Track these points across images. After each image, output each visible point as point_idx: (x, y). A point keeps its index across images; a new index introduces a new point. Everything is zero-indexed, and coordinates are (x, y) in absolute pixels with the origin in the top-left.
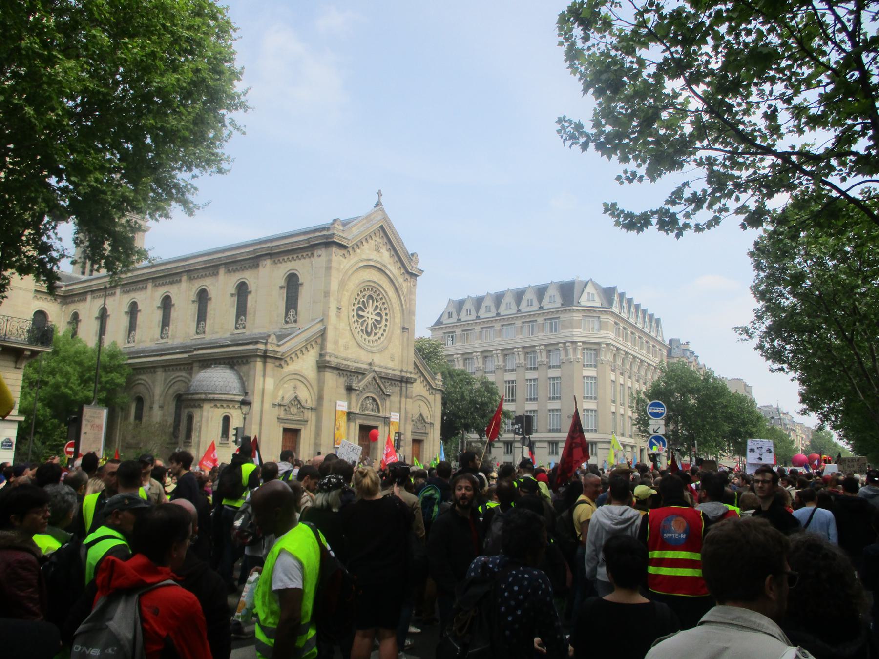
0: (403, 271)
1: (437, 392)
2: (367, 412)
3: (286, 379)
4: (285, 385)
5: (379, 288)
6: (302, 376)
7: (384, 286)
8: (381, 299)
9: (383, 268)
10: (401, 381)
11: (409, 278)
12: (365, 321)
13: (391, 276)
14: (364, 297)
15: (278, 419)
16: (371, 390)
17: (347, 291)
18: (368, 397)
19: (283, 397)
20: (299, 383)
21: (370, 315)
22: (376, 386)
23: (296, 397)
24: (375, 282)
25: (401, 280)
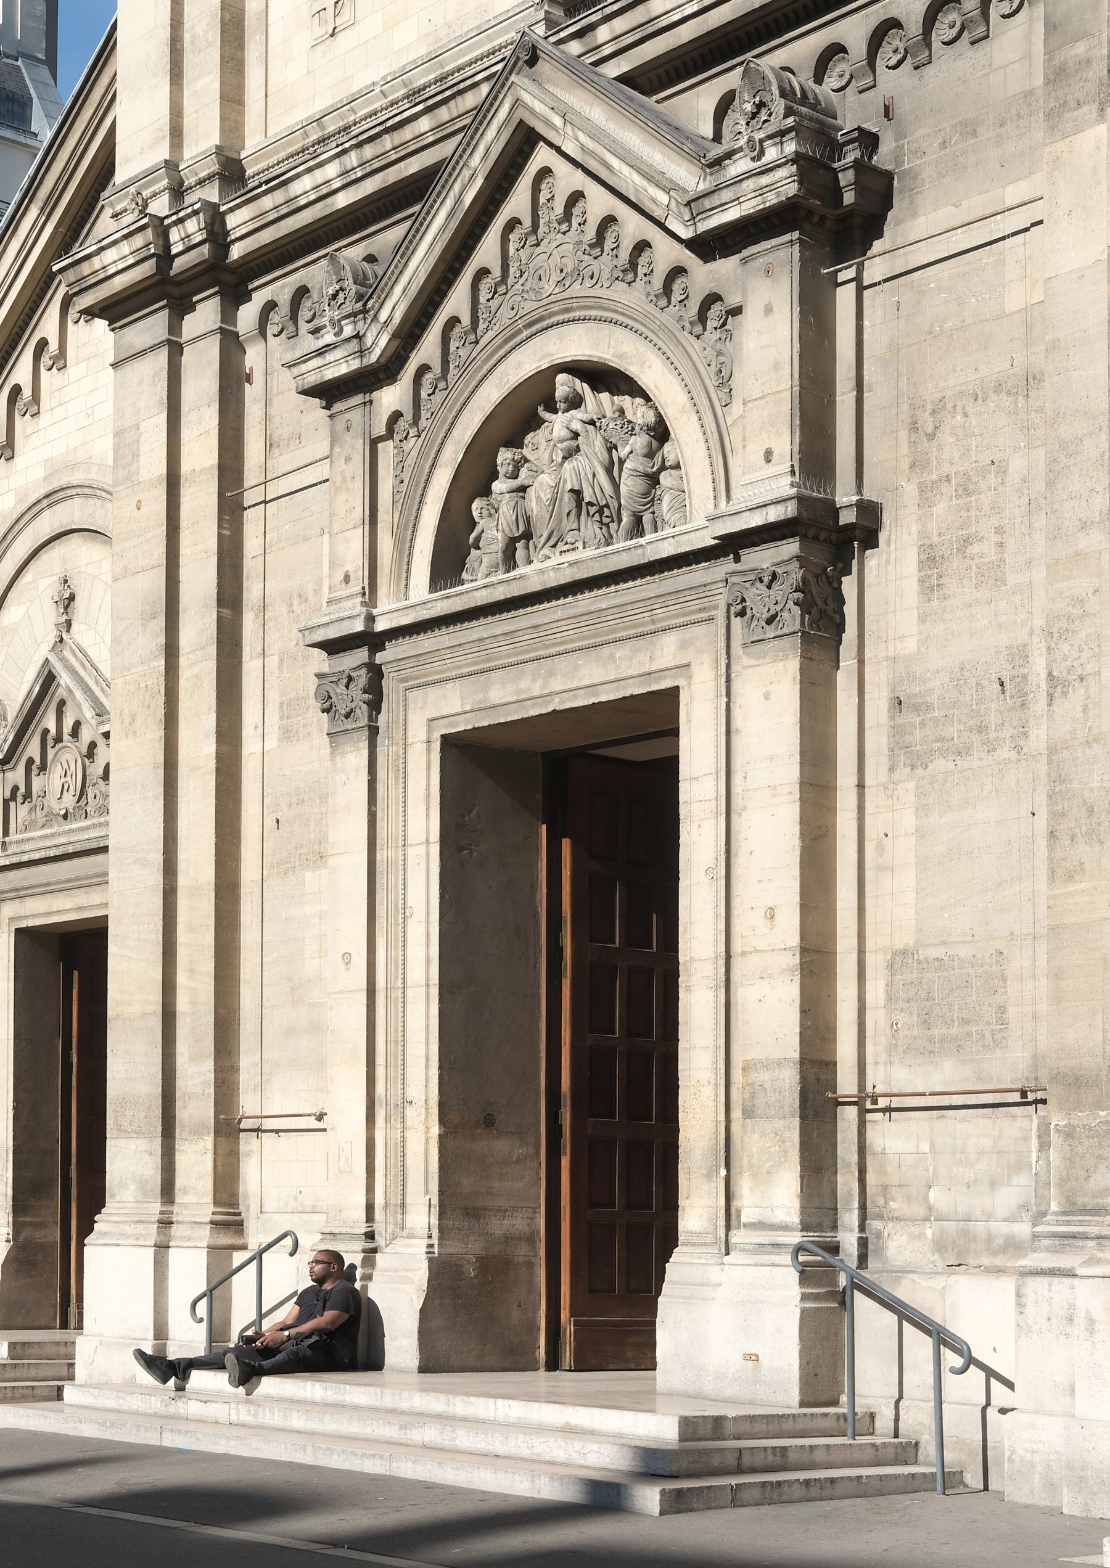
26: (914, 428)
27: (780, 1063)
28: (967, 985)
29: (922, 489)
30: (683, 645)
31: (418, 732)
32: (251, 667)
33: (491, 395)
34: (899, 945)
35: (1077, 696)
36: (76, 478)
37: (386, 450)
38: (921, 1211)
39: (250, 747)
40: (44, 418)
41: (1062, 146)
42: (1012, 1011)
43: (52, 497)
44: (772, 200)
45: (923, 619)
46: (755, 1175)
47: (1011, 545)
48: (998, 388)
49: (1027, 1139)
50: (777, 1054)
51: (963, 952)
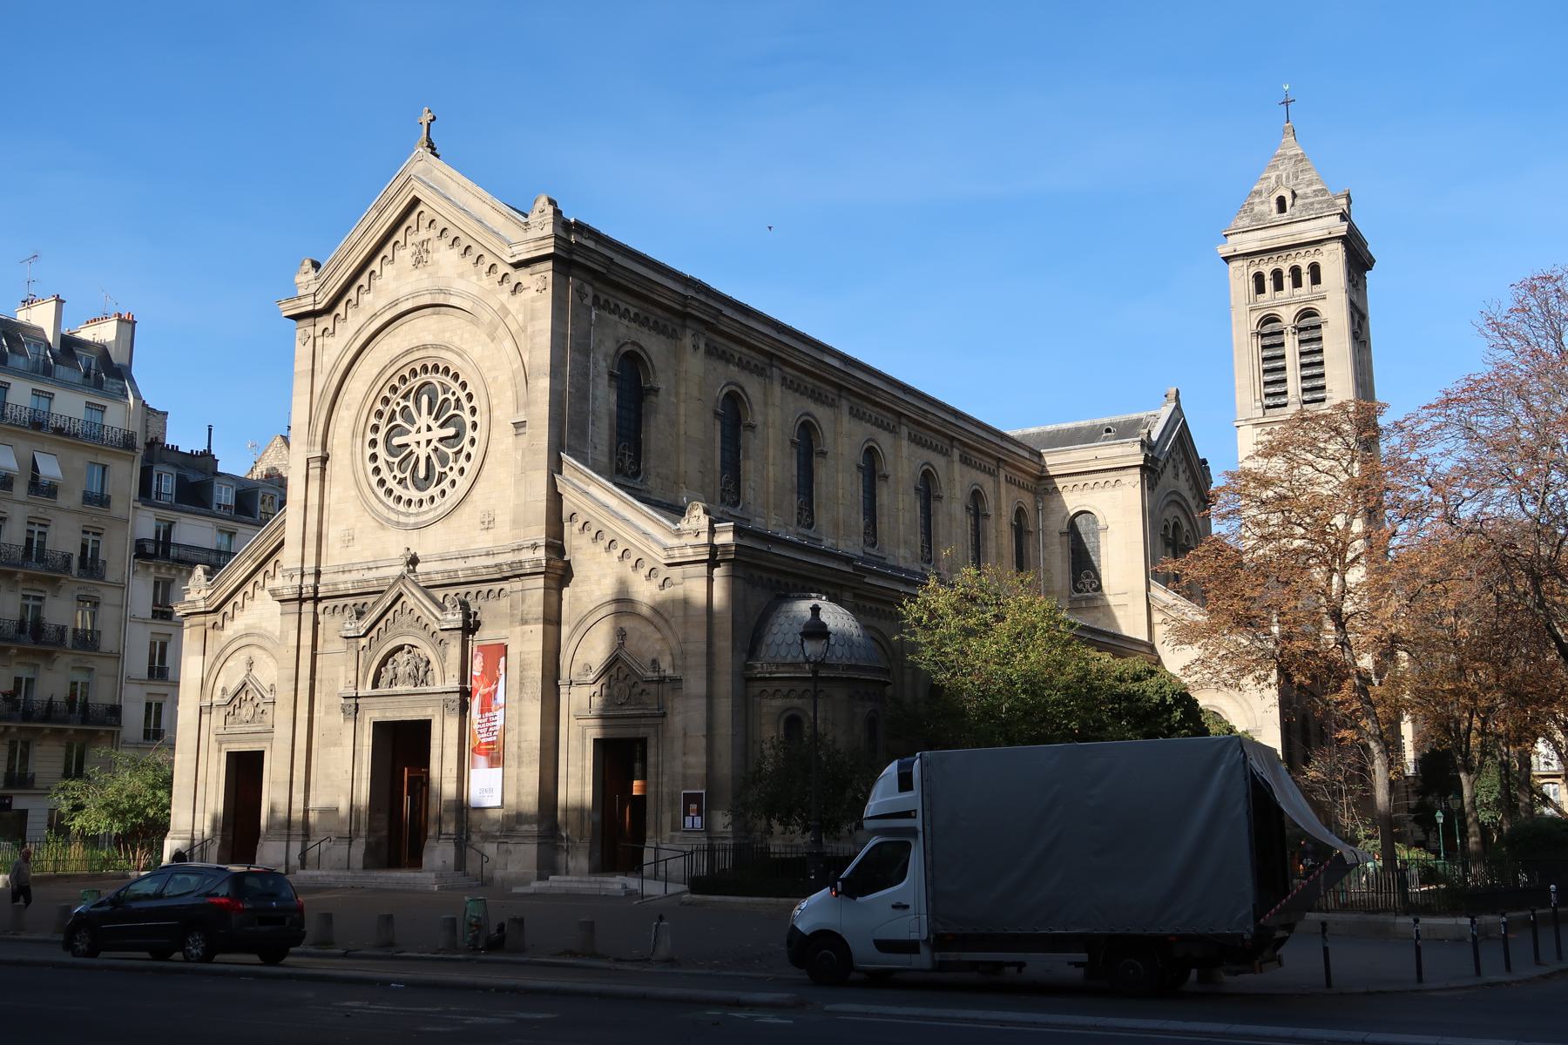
1: (690, 569)
2: (399, 688)
3: (229, 651)
4: (229, 664)
6: (261, 636)
7: (456, 342)
9: (440, 299)
12: (411, 453)
17: (348, 407)
18: (401, 648)
20: (256, 652)
21: (423, 434)
24: (425, 347)
30: (433, 711)
31: (367, 720)
35: (512, 732)
36: (256, 631)
39: (316, 715)
40: (245, 612)
41: (512, 629)
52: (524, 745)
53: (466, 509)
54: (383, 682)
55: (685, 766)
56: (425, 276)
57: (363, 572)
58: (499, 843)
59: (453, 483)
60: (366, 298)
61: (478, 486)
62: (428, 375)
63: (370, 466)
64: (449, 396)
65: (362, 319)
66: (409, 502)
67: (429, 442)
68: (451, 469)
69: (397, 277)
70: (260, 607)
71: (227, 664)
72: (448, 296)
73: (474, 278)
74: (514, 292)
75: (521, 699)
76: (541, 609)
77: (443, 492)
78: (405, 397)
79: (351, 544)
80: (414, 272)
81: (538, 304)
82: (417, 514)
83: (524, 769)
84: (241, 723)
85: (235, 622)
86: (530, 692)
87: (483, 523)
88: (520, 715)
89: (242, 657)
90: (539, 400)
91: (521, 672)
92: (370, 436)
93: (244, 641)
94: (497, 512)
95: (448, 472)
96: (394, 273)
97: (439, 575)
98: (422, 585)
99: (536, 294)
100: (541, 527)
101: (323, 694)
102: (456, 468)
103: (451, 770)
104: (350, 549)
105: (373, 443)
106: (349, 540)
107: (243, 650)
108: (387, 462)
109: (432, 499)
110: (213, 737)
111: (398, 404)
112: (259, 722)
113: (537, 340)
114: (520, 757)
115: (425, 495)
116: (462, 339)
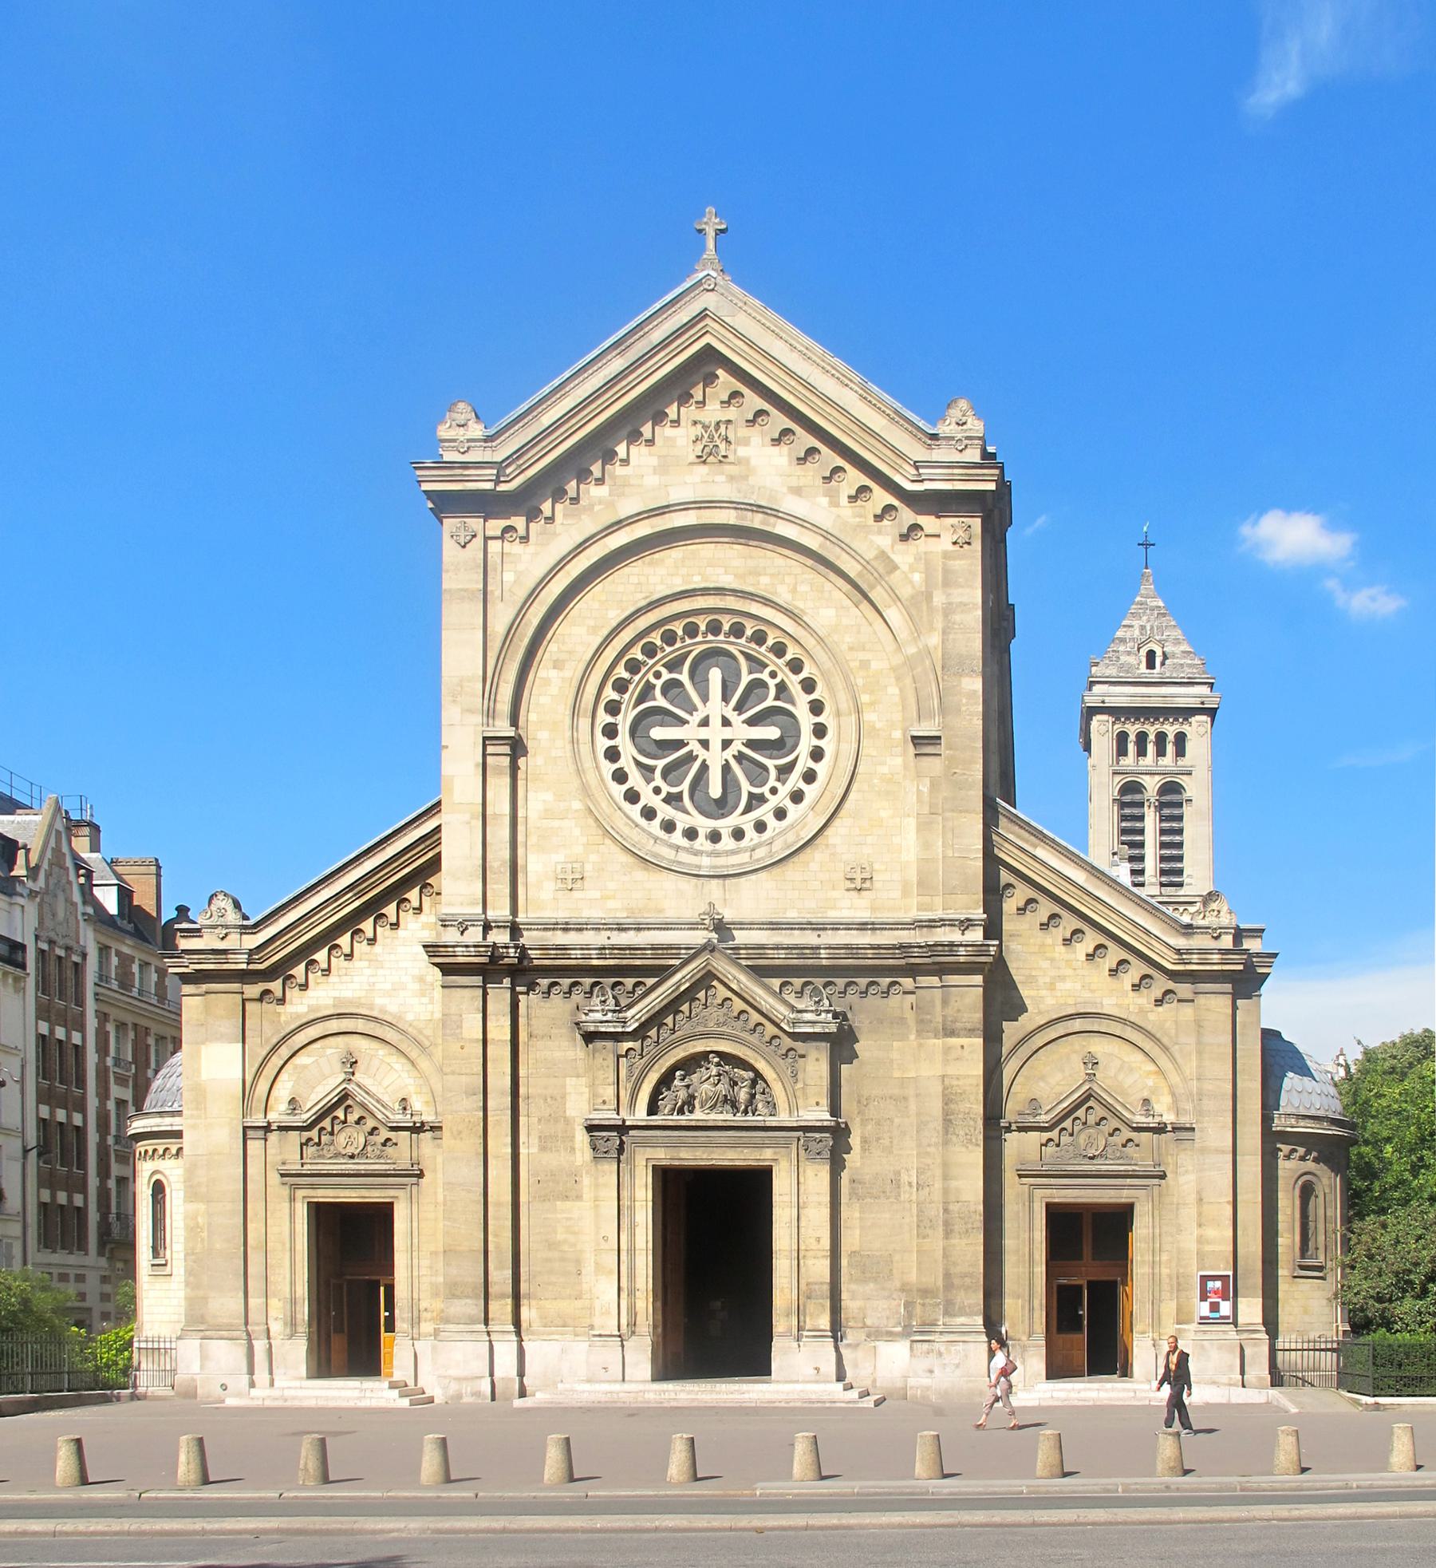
0: (881, 497)
2: (699, 1116)
4: (299, 1060)
5: (755, 608)
6: (375, 1019)
7: (783, 596)
8: (779, 650)
9: (756, 521)
10: (913, 971)
11: (928, 522)
12: (691, 758)
13: (812, 541)
14: (674, 665)
15: (282, 1175)
16: (712, 1027)
17: (557, 665)
18: (705, 1055)
19: (292, 1101)
22: (739, 1005)
23: (345, 1096)
24: (720, 591)
25: (884, 538)
26: (859, 1102)
27: (821, 1283)
28: (878, 1263)
29: (862, 1120)
30: (775, 1153)
31: (640, 1162)
32: (522, 1120)
33: (679, 1053)
34: (854, 1250)
37: (623, 1060)
38: (860, 1325)
39: (523, 1150)
40: (332, 978)
42: (894, 1271)
43: (340, 1016)
44: (827, 1030)
45: (861, 1158)
46: (811, 1315)
47: (895, 1142)
48: (891, 1098)
49: (900, 1305)
50: (821, 1280)
51: (878, 1254)
52: (953, 1207)
53: (815, 857)
54: (665, 1105)
55: (1200, 1240)
56: (722, 478)
57: (608, 933)
58: (913, 1341)
59: (780, 814)
60: (594, 492)
61: (837, 822)
62: (721, 637)
63: (608, 768)
64: (765, 676)
65: (591, 528)
66: (691, 834)
67: (726, 744)
68: (774, 791)
69: (662, 469)
70: (368, 972)
71: (296, 1060)
72: (772, 520)
73: (824, 501)
74: (904, 537)
75: (946, 1143)
76: (979, 1015)
77: (760, 827)
78: (674, 665)
79: (579, 884)
80: (695, 467)
81: (957, 565)
82: (711, 854)
83: (953, 1241)
84: (337, 1155)
85: (309, 993)
86: (962, 1133)
87: (851, 880)
88: (945, 1165)
89: (329, 1051)
90: (964, 709)
91: (946, 1104)
92: (604, 718)
93: (334, 1026)
94: (876, 866)
95: (768, 795)
96: (654, 461)
97: (783, 951)
98: (749, 963)
99: (952, 548)
100: (976, 897)
101: (534, 1120)
102: (784, 790)
103: (818, 1240)
104: (576, 894)
105: (610, 731)
106: (573, 881)
107: (340, 1039)
108: (638, 763)
109: (738, 834)
110: (274, 1178)
111: (658, 675)
112: (379, 1157)
113: (957, 618)
114: (946, 1223)
115: (725, 825)
116: (794, 591)
